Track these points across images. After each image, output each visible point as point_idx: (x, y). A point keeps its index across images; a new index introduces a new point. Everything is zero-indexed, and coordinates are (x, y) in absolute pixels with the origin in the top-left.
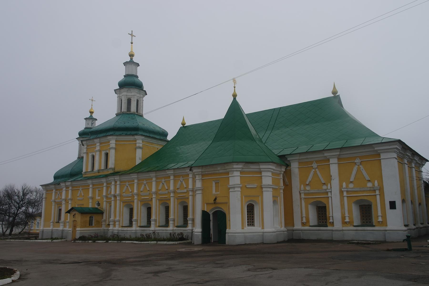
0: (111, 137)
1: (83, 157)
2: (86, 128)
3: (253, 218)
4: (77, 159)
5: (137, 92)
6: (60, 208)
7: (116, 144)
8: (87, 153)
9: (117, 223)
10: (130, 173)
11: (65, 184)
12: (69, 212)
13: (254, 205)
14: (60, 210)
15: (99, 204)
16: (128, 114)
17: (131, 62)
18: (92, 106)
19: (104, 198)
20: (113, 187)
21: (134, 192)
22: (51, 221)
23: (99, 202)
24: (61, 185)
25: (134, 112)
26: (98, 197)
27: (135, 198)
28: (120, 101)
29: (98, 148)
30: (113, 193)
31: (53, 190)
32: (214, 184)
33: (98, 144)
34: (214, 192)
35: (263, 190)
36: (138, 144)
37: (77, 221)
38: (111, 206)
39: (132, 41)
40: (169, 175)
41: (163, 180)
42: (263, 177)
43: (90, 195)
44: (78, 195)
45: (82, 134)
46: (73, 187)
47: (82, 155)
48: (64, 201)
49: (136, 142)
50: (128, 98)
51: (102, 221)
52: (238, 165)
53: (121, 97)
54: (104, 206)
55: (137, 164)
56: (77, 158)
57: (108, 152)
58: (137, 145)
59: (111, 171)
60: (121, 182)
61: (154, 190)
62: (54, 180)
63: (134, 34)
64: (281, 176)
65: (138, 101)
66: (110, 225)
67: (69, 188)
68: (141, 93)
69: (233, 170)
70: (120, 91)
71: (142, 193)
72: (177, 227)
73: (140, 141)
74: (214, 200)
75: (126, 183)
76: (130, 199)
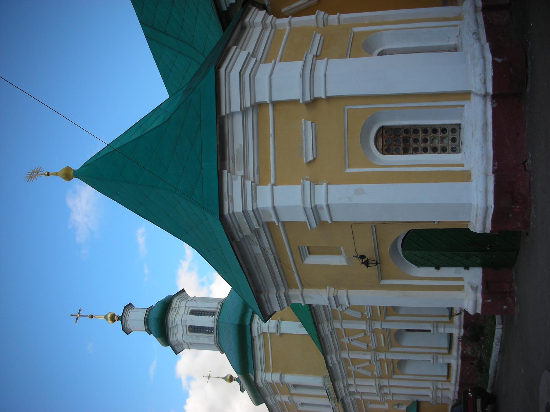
3: (430, 131)
5: (175, 313)
13: (382, 128)
16: (218, 334)
18: (219, 378)
19: (386, 399)
29: (285, 398)
32: (311, 260)
34: (339, 260)
35: (323, 97)
36: (270, 329)
39: (87, 316)
42: (275, 99)
50: (189, 330)
52: (232, 197)
61: (363, 326)
63: (76, 312)
64: (282, 22)
65: (194, 313)
68: (177, 306)
69: (251, 214)
71: (373, 345)
74: (368, 266)
75: (351, 370)
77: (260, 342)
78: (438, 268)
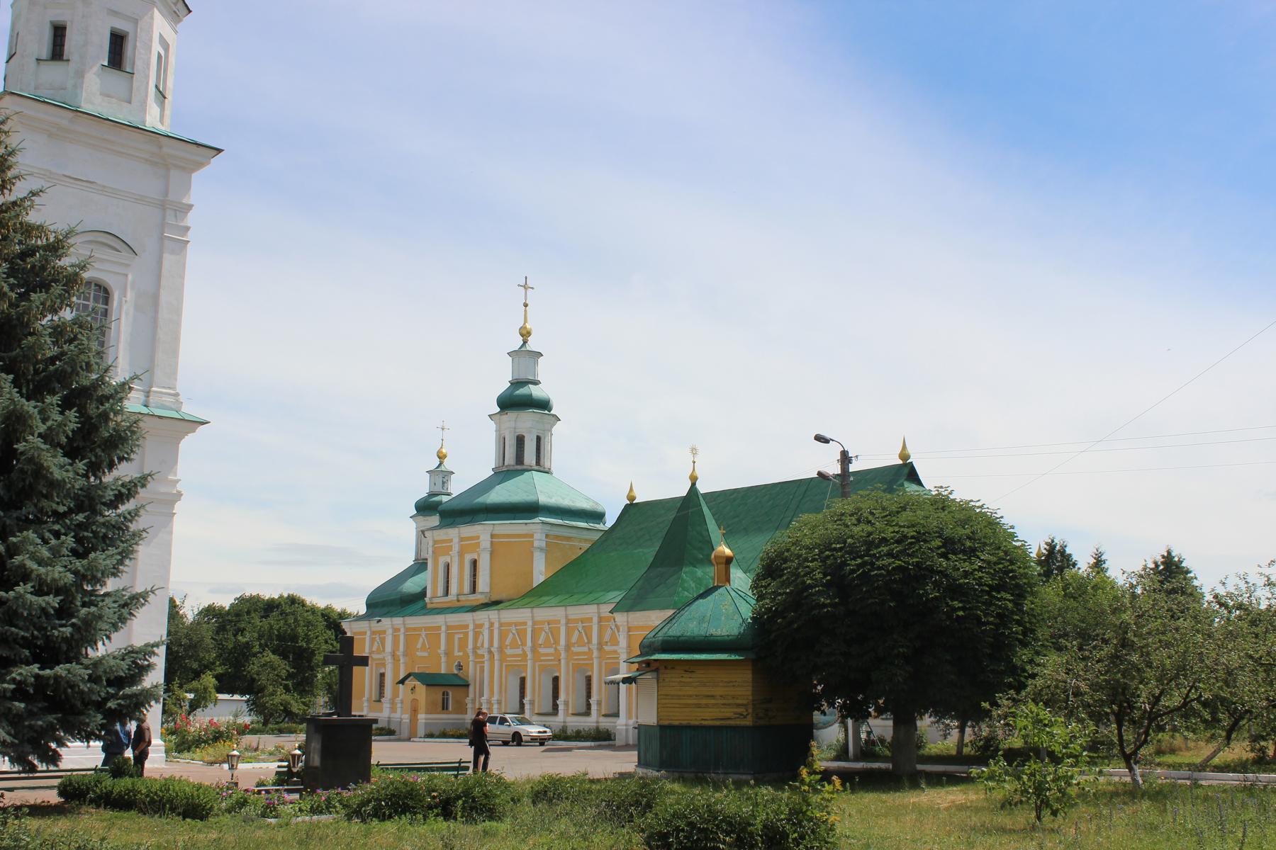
1: (427, 559)
4: (413, 563)
6: (382, 671)
12: (402, 682)
14: (382, 675)
15: (460, 667)
22: (365, 699)
23: (459, 662)
28: (502, 443)
33: (456, 540)
37: (417, 700)
41: (580, 625)
44: (419, 646)
45: (425, 507)
47: (424, 555)
48: (390, 657)
54: (471, 671)
65: (539, 439)
67: (399, 630)
71: (542, 651)
72: (605, 716)
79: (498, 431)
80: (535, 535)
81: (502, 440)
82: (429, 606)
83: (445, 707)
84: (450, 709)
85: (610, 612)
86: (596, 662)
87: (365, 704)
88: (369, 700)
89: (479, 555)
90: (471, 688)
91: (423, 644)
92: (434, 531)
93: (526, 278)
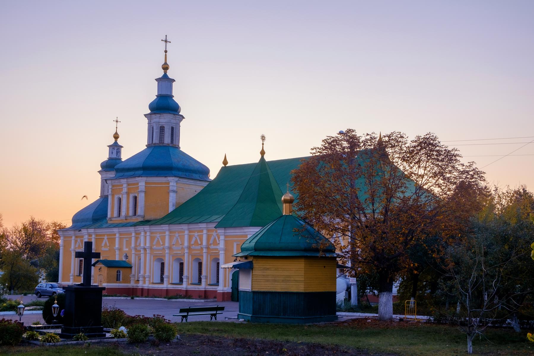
0: (140, 178)
2: (110, 159)
5: (172, 118)
7: (145, 186)
8: (113, 195)
9: (147, 279)
10: (161, 224)
11: (88, 231)
15: (127, 257)
17: (165, 77)
20: (142, 238)
21: (165, 245)
22: (71, 274)
23: (126, 254)
24: (83, 232)
25: (168, 144)
26: (126, 248)
27: (166, 252)
30: (142, 245)
31: (71, 237)
33: (125, 185)
38: (140, 259)
40: (202, 228)
43: (117, 246)
46: (96, 235)
47: (106, 194)
49: (169, 184)
51: (130, 276)
53: (152, 124)
54: (133, 260)
55: (170, 212)
56: (99, 197)
57: (136, 195)
58: (171, 188)
59: (140, 219)
60: (151, 233)
62: (73, 224)
63: (168, 40)
65: (172, 129)
66: (139, 281)
68: (176, 118)
70: (150, 117)
73: (172, 182)
76: (161, 253)
77: (164, 180)
78: (232, 280)
79: (149, 123)
80: (170, 183)
81: (151, 129)
82: (109, 222)
83: (118, 279)
84: (121, 280)
85: (214, 227)
86: (205, 255)
87: (71, 277)
88: (74, 276)
89: (138, 194)
90: (133, 268)
91: (106, 244)
92: (112, 180)
93: (166, 36)
